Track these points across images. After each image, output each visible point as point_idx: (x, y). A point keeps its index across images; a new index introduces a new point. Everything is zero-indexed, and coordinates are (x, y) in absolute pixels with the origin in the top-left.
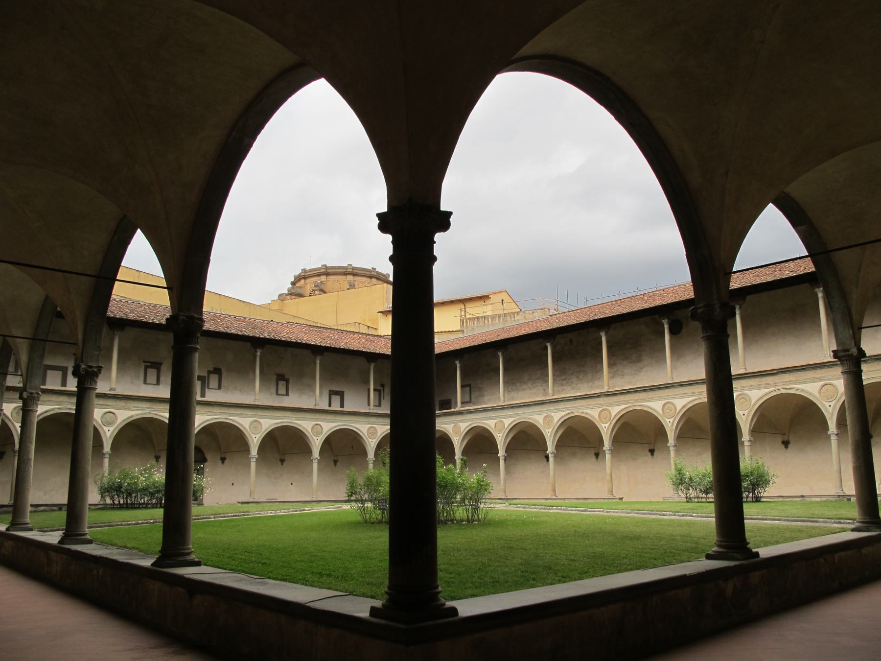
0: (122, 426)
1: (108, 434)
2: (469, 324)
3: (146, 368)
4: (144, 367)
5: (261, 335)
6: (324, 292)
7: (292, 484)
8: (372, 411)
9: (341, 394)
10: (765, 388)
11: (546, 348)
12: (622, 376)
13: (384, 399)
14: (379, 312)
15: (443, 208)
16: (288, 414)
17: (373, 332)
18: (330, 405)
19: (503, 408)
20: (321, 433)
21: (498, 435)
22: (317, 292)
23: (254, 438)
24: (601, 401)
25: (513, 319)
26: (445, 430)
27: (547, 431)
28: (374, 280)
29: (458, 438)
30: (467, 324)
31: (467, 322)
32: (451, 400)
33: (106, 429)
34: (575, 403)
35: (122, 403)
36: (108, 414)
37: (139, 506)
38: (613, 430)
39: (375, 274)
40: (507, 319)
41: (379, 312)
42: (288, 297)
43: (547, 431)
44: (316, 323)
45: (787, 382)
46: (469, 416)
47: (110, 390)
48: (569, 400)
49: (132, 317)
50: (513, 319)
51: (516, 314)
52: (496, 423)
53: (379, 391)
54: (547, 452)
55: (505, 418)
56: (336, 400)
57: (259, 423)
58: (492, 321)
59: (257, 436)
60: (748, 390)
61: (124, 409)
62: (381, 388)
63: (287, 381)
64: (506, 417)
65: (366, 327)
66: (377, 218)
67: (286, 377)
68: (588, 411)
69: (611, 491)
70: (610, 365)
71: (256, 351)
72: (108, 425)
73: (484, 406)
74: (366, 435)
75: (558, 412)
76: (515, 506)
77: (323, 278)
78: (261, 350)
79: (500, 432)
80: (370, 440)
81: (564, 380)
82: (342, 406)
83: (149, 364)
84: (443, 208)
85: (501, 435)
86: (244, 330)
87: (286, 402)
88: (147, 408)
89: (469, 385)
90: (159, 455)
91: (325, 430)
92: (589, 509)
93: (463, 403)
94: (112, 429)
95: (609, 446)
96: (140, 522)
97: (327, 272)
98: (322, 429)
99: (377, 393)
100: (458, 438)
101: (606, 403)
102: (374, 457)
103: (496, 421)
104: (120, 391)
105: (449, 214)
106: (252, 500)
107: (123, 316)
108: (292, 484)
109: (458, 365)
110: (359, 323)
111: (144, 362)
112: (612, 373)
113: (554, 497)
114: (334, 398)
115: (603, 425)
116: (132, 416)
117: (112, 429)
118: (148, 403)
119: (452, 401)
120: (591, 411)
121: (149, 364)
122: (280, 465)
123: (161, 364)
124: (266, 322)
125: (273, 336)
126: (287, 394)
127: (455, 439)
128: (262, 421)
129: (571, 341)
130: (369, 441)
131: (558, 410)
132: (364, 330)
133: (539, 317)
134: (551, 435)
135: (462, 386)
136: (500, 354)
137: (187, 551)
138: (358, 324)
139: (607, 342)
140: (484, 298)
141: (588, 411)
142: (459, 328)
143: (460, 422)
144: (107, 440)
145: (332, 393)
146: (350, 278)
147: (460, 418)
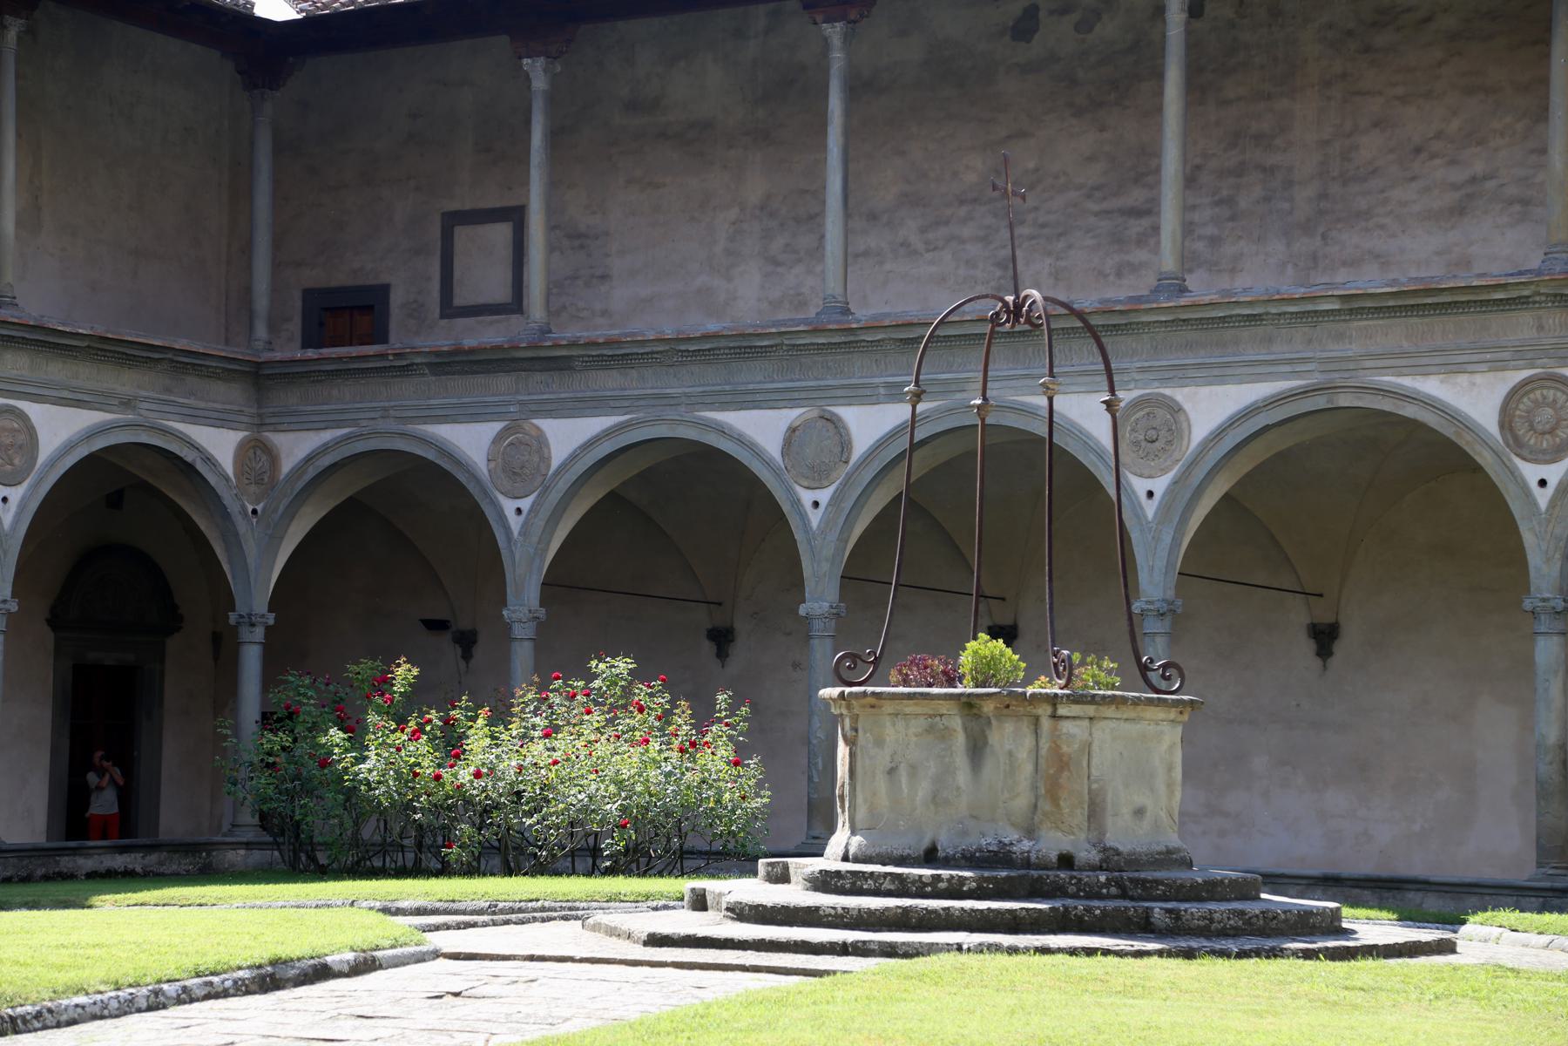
12: (1517, 208)
29: (525, 504)
32: (385, 290)
34: (1340, 337)
46: (609, 381)
52: (792, 430)
55: (849, 401)
64: (864, 396)
68: (1431, 386)
75: (1221, 380)
79: (817, 478)
85: (824, 496)
100: (525, 504)
103: (789, 416)
109: (539, 83)
112: (1455, 187)
115: (1531, 472)
127: (509, 506)
131: (1219, 374)
141: (1431, 386)
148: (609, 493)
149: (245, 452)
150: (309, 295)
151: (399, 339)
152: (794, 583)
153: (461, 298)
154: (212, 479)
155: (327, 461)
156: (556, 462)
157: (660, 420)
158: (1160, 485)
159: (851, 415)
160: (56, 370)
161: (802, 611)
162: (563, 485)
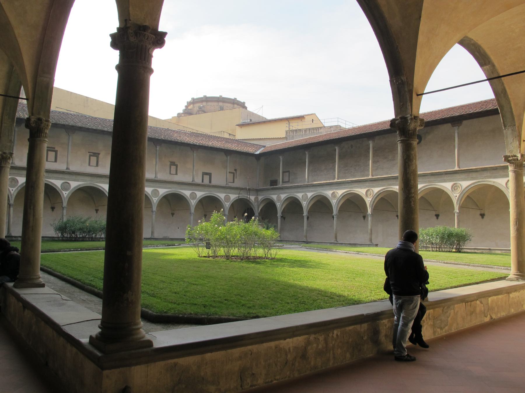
0: (73, 191)
1: (65, 195)
2: (291, 134)
3: (90, 156)
4: (88, 156)
5: (159, 137)
6: (205, 112)
7: (178, 228)
8: (227, 186)
9: (210, 174)
10: (471, 180)
11: (335, 150)
13: (236, 178)
14: (237, 125)
15: (160, 29)
16: (176, 186)
17: (232, 137)
18: (203, 181)
19: (307, 186)
20: (196, 198)
21: (304, 203)
22: (200, 112)
23: (154, 200)
24: (367, 184)
25: (318, 131)
26: (272, 198)
27: (334, 201)
28: (236, 106)
29: (279, 204)
30: (289, 134)
31: (289, 132)
33: (64, 192)
34: (351, 185)
35: (74, 177)
36: (65, 183)
37: (76, 240)
38: (374, 202)
39: (236, 102)
40: (314, 131)
41: (237, 125)
42: (183, 115)
43: (334, 201)
44: (198, 131)
45: (485, 177)
46: (287, 191)
47: (66, 169)
48: (348, 182)
49: (80, 125)
50: (318, 131)
51: (320, 128)
52: (303, 195)
53: (234, 173)
54: (333, 214)
56: (207, 178)
57: (158, 191)
58: (305, 132)
59: (156, 199)
60: (459, 181)
61: (75, 180)
62: (235, 172)
63: (177, 166)
64: (309, 192)
65: (228, 134)
66: (110, 38)
67: (176, 163)
68: (359, 190)
69: (371, 240)
70: (373, 162)
71: (156, 147)
72: (66, 190)
73: (296, 185)
74: (224, 200)
76: (305, 248)
77: (204, 104)
78: (159, 147)
79: (305, 201)
80: (226, 203)
81: (346, 170)
82: (210, 182)
83: (92, 154)
84: (160, 29)
85: (305, 203)
86: (149, 134)
87: (176, 178)
88: (89, 180)
89: (289, 172)
90: (98, 209)
91: (198, 197)
92: (349, 252)
93: (283, 182)
94: (67, 192)
95: (371, 212)
96: (72, 250)
97: (206, 100)
98: (196, 196)
99: (232, 174)
100: (279, 204)
101: (370, 186)
102: (228, 213)
103: (303, 194)
104: (73, 168)
105: (164, 34)
106: (152, 237)
107: (74, 124)
108: (178, 228)
110: (224, 132)
111: (89, 152)
113: (336, 242)
114: (205, 176)
116: (80, 185)
117: (67, 192)
118: (90, 177)
119: (278, 181)
120: (361, 191)
121: (92, 154)
122: (171, 216)
123: (99, 154)
124: (164, 129)
125: (167, 138)
126: (176, 174)
127: (278, 204)
128: (159, 190)
129: (352, 146)
130: (225, 203)
132: (226, 136)
133: (334, 131)
134: (336, 203)
135: (283, 172)
136: (307, 153)
137: (35, 277)
138: (223, 132)
139: (373, 148)
140: (301, 118)
142: (284, 136)
143: (282, 194)
144: (64, 199)
145: (204, 174)
146: (221, 104)
147: (281, 191)
148: (347, 199)
149: (256, 199)
150: (271, 181)
151: (280, 185)
152: (277, 213)
153: (284, 181)
154: (251, 201)
155: (262, 199)
156: (282, 199)
157: (290, 195)
158: (335, 201)
159: (308, 194)
160: (233, 191)
161: (303, 215)
162: (283, 201)
